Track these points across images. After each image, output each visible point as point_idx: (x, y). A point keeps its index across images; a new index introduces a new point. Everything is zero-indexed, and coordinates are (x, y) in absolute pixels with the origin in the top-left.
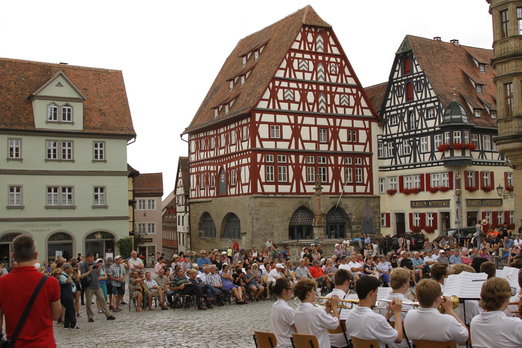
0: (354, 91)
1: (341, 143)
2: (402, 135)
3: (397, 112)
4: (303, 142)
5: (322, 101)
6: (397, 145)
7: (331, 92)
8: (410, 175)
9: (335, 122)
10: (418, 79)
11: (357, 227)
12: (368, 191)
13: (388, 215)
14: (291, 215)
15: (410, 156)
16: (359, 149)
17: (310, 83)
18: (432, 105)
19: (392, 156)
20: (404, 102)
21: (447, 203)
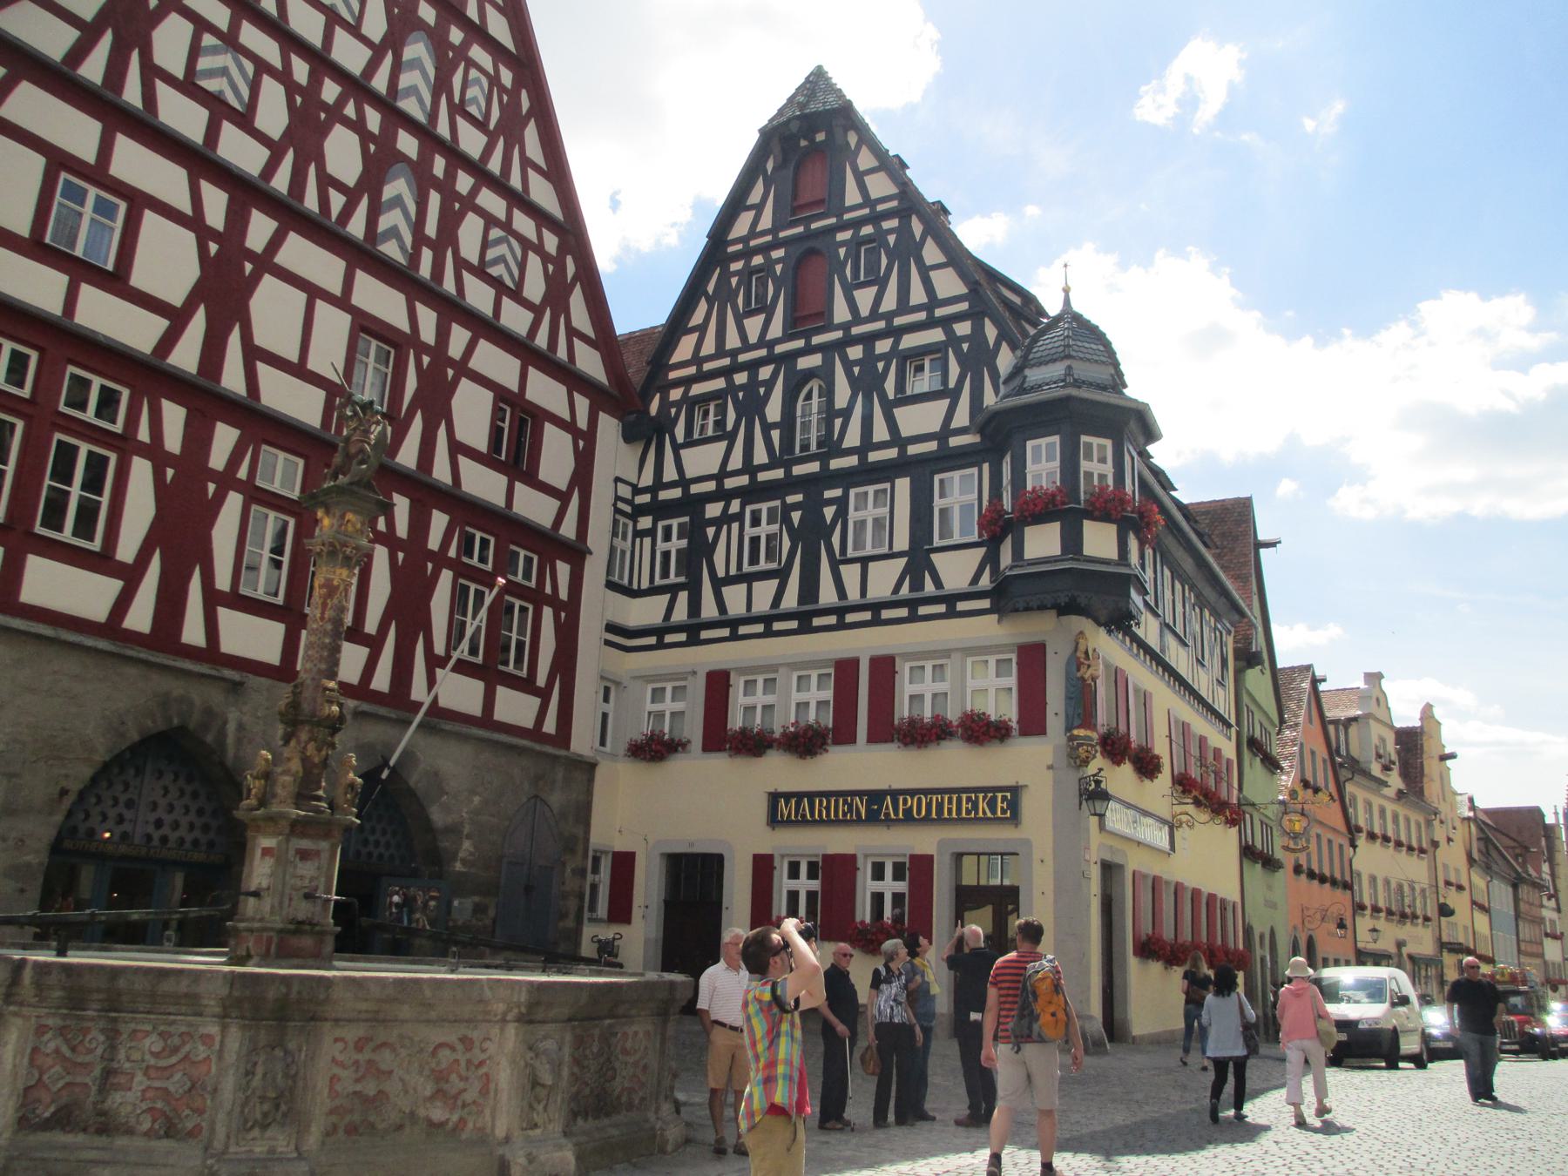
0: (551, 242)
1: (457, 448)
2: (744, 480)
3: (730, 381)
4: (253, 355)
5: (397, 201)
6: (711, 531)
7: (446, 187)
8: (773, 668)
9: (443, 334)
10: (867, 230)
11: (479, 909)
12: (550, 726)
13: (624, 863)
14: (87, 772)
15: (782, 575)
16: (534, 507)
17: (356, 87)
18: (936, 335)
19: (673, 578)
20: (776, 330)
21: (1009, 802)
